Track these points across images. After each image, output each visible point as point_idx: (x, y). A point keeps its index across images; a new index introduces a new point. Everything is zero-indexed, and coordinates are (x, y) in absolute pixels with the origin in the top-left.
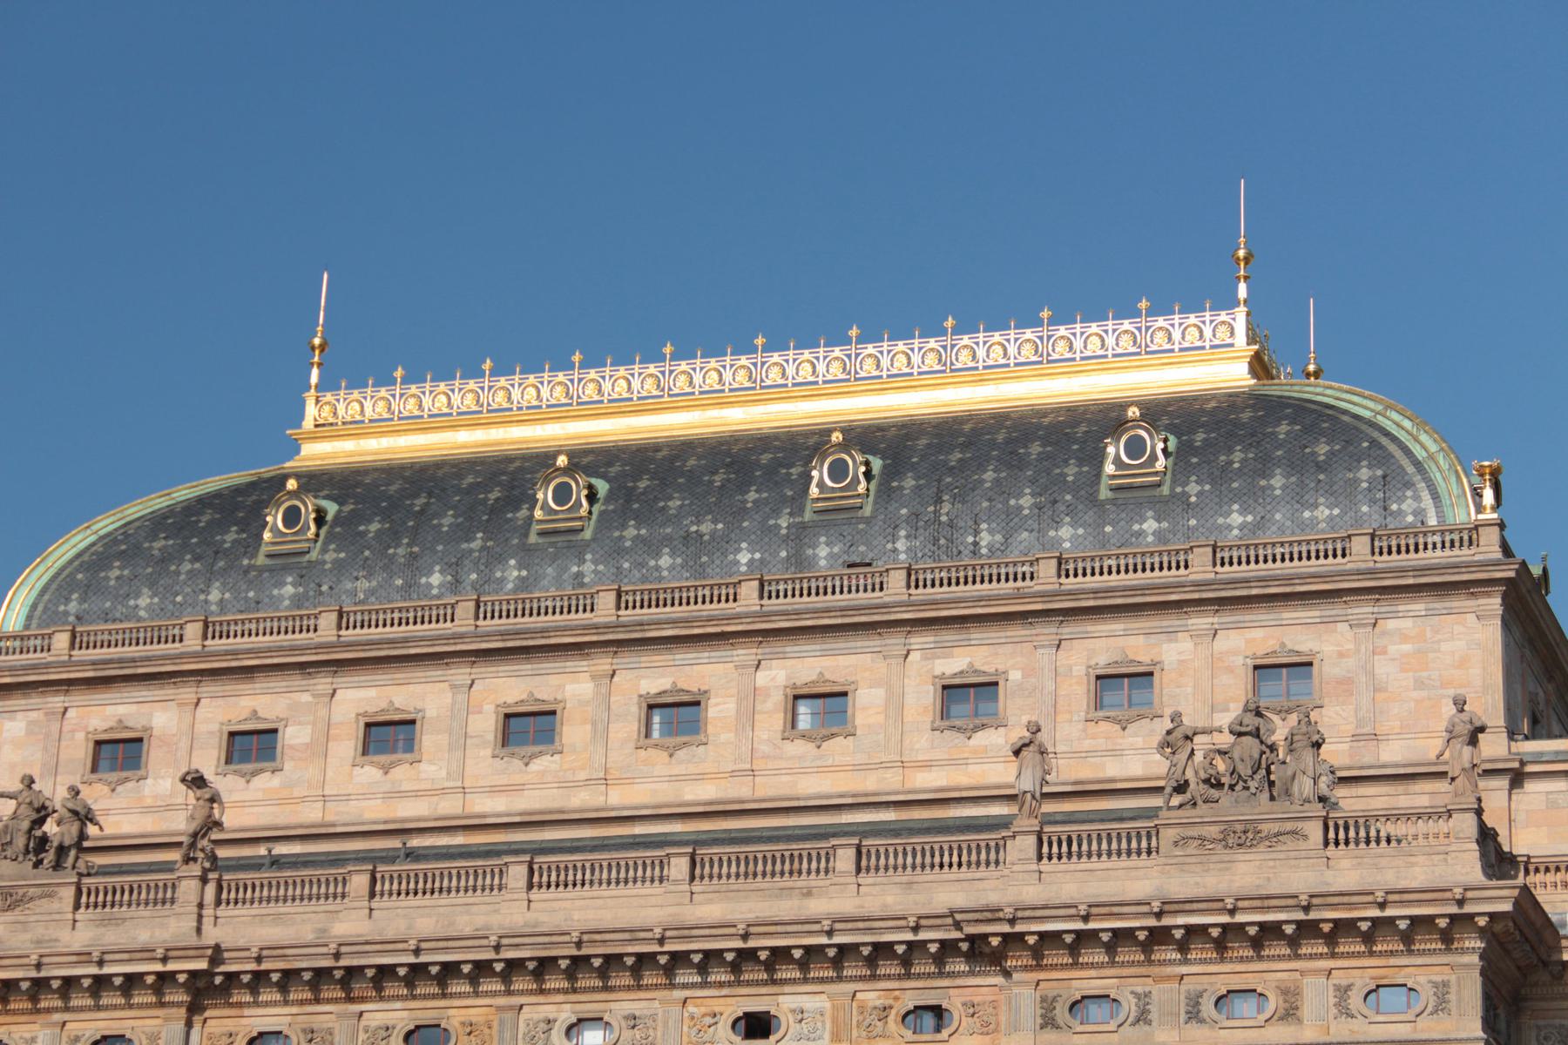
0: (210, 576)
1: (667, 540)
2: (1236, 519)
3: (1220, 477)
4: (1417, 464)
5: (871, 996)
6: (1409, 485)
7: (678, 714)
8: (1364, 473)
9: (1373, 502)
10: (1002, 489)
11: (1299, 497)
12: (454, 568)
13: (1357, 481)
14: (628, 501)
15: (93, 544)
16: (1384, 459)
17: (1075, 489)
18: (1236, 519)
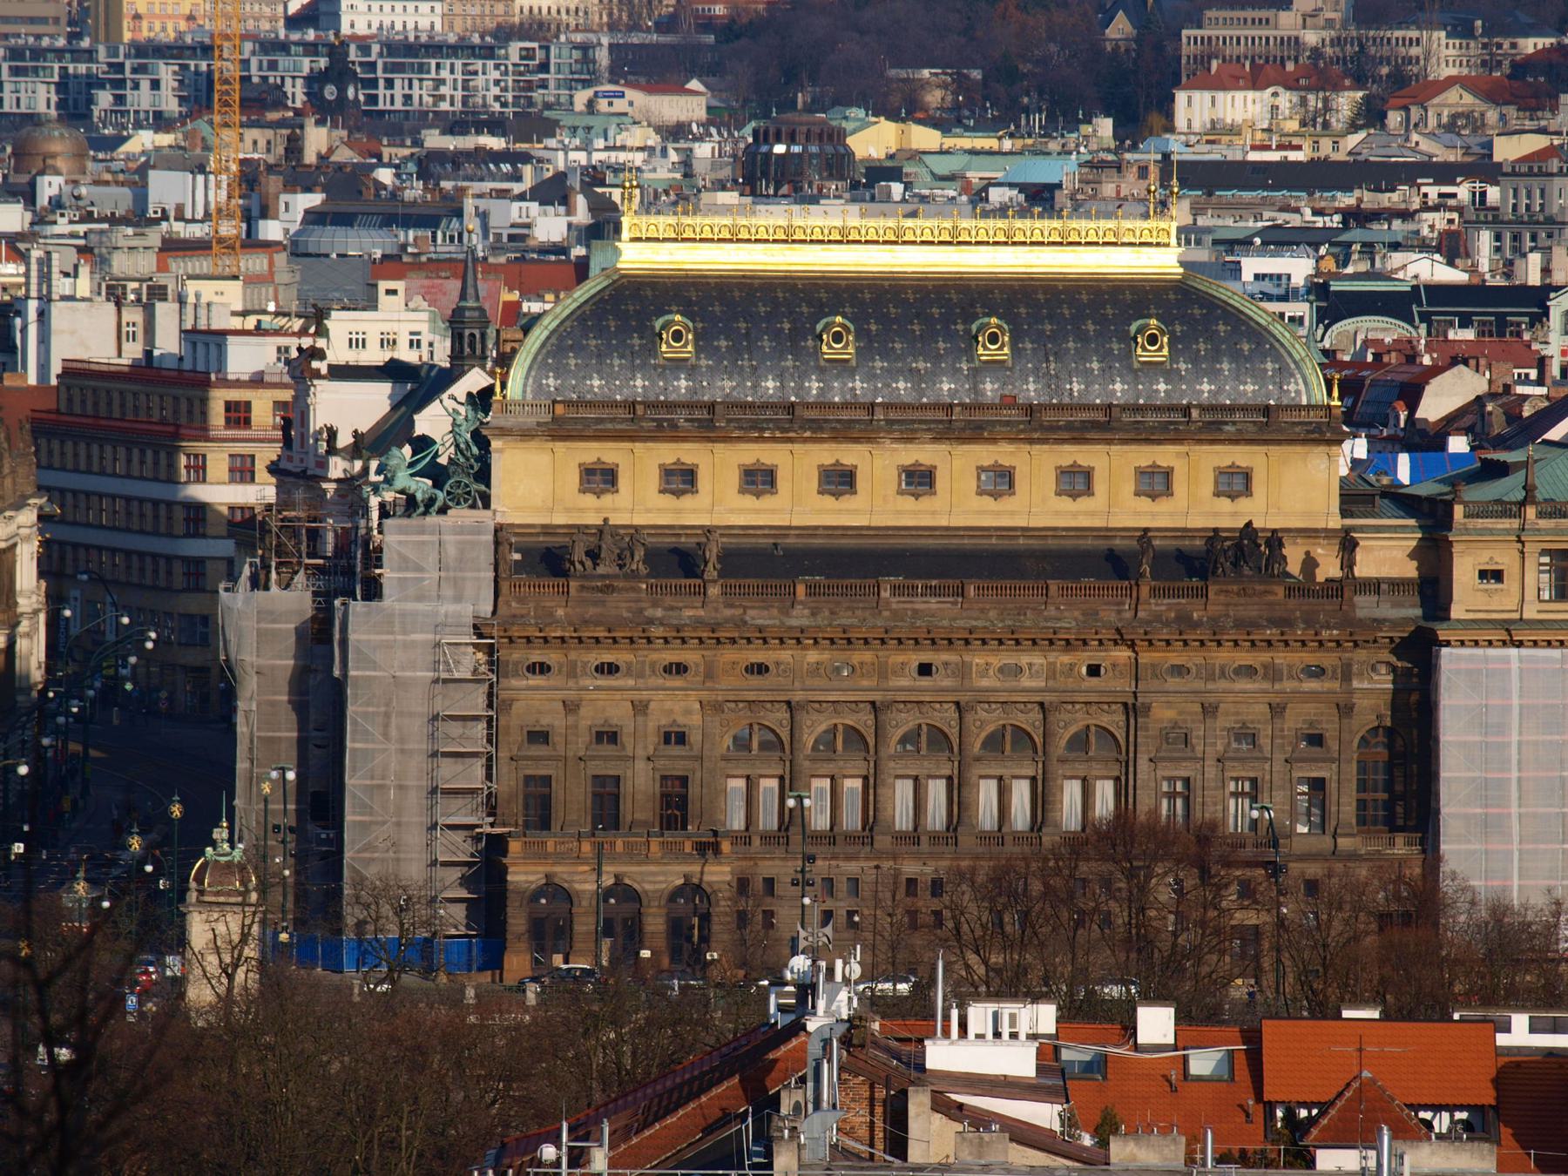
0: (633, 369)
1: (900, 371)
2: (1206, 387)
3: (1195, 359)
4: (1295, 362)
5: (1066, 659)
6: (1292, 375)
7: (920, 480)
8: (1269, 366)
9: (1274, 384)
10: (1083, 357)
11: (1238, 378)
12: (780, 377)
13: (1266, 370)
14: (870, 341)
15: (548, 338)
16: (1277, 358)
17: (1120, 359)
18: (1206, 387)
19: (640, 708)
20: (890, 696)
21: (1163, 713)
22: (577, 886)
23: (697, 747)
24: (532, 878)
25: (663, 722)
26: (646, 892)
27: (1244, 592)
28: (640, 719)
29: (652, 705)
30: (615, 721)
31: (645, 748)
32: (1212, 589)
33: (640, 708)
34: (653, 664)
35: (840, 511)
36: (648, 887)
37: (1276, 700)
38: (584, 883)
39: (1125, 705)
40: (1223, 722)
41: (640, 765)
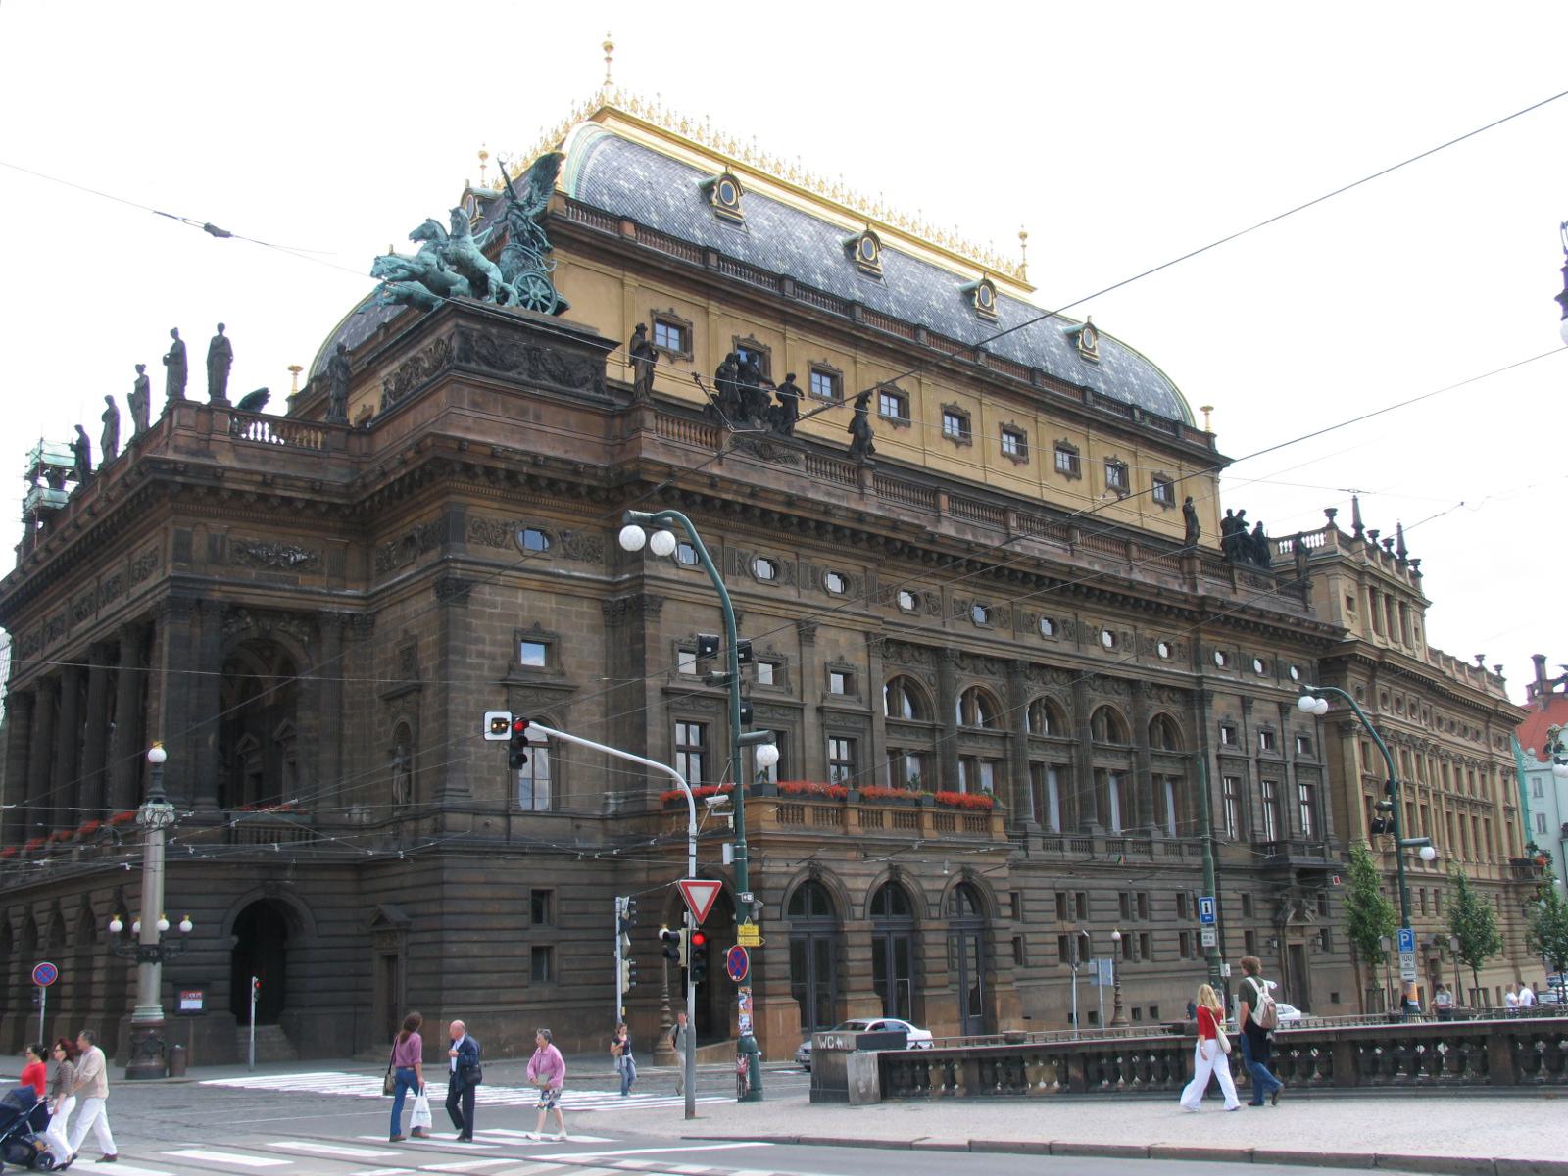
5: (1148, 633)
19: (806, 633)
20: (1026, 658)
21: (1221, 707)
22: (849, 883)
23: (865, 698)
24: (794, 868)
25: (829, 659)
26: (924, 892)
27: (1255, 583)
28: (806, 649)
29: (819, 631)
30: (779, 649)
31: (814, 693)
32: (1236, 573)
33: (806, 633)
34: (815, 571)
35: (898, 443)
36: (926, 885)
37: (1284, 700)
38: (858, 880)
39: (1184, 691)
40: (1255, 719)
41: (810, 717)
